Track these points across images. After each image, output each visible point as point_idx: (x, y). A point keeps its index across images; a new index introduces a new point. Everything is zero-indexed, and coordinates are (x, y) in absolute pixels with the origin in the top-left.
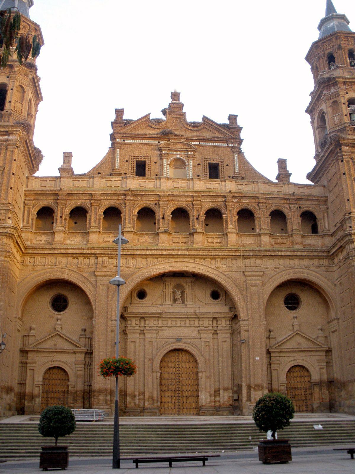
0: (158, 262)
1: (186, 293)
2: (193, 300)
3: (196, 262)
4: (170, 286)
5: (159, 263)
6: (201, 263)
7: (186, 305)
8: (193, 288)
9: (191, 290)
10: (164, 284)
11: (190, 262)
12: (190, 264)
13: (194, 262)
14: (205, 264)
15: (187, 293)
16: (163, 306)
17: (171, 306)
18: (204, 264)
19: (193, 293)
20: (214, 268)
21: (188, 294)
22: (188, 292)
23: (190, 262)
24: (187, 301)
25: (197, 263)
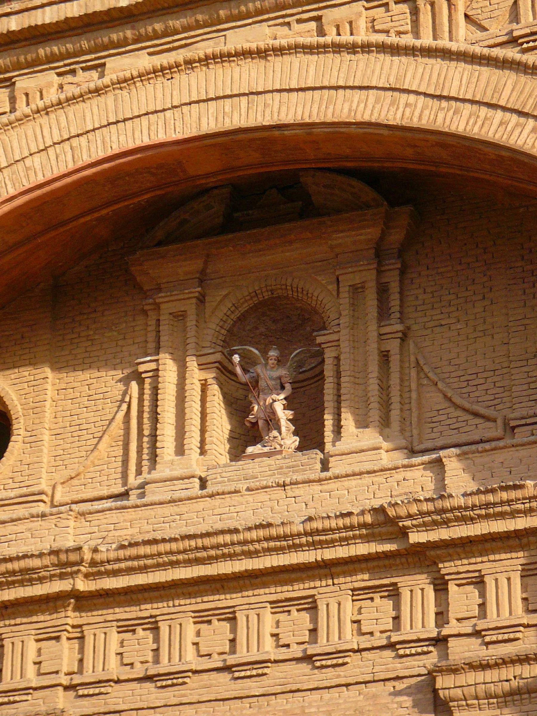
0: (13, 110)
1: (329, 355)
2: (395, 414)
3: (331, 37)
4: (191, 322)
5: (22, 108)
6: (380, 38)
7: (325, 466)
8: (395, 302)
9: (373, 327)
10: (152, 322)
11: (280, 51)
12: (276, 62)
13: (315, 40)
14: (417, 34)
15: (338, 358)
16: (133, 499)
17: (196, 490)
18: (408, 40)
19: (393, 346)
20: (497, 52)
21: (345, 366)
22: (345, 346)
23: (280, 51)
24: (338, 429)
25: (346, 38)
